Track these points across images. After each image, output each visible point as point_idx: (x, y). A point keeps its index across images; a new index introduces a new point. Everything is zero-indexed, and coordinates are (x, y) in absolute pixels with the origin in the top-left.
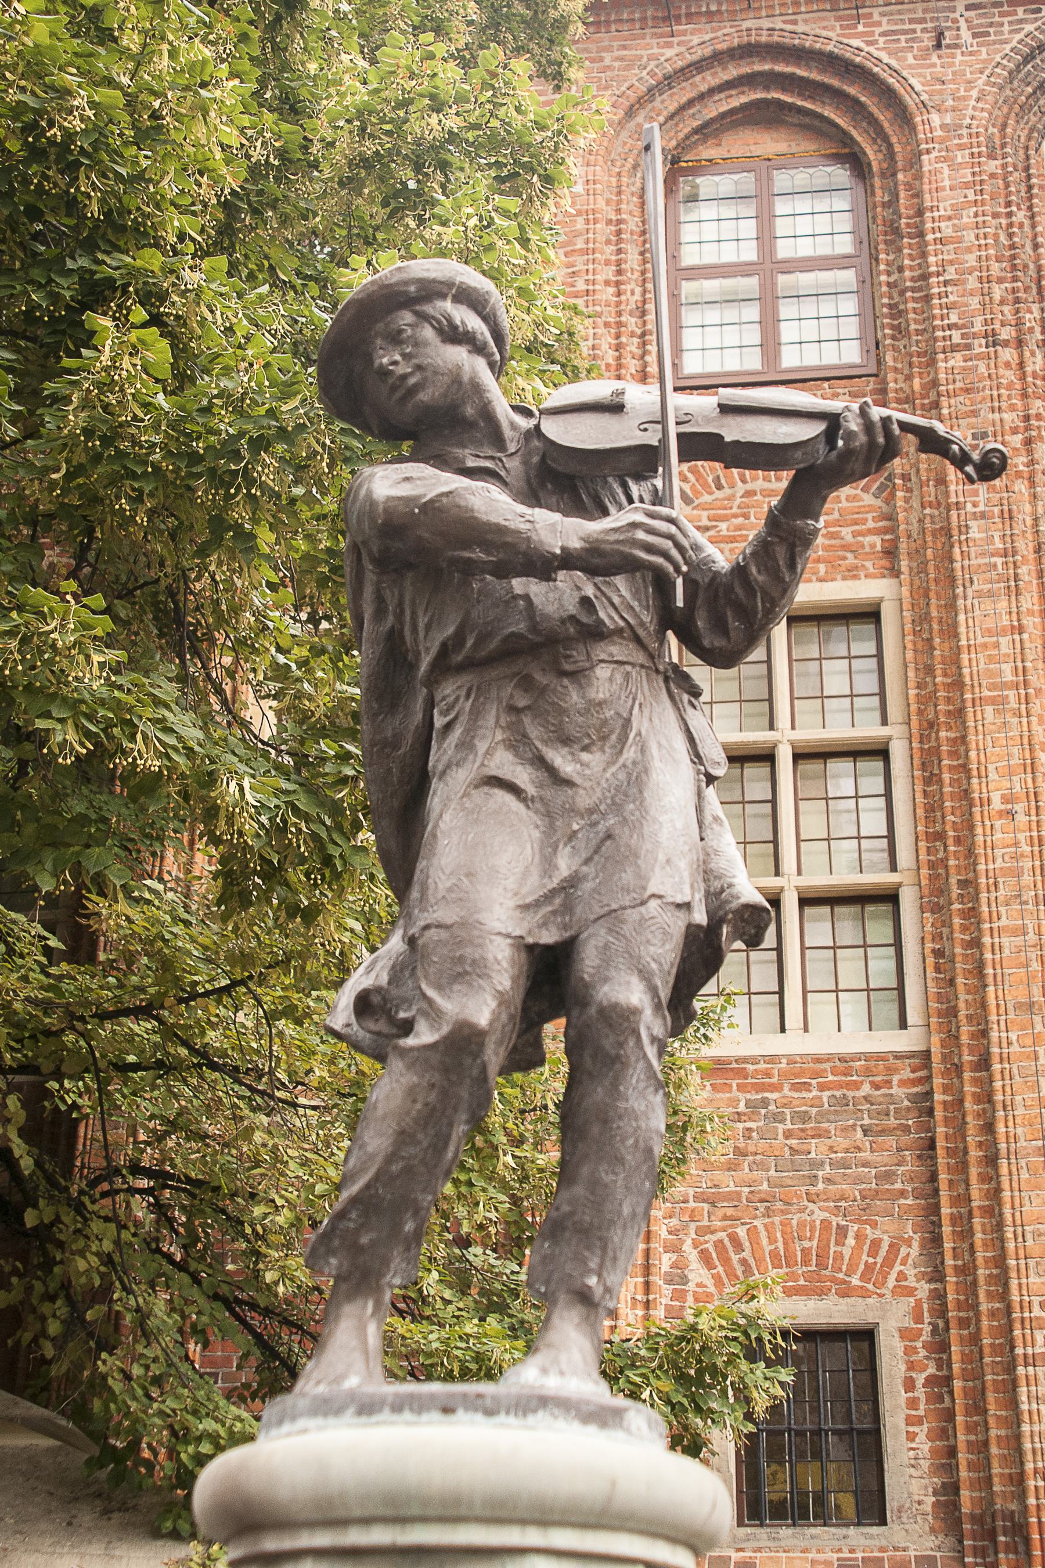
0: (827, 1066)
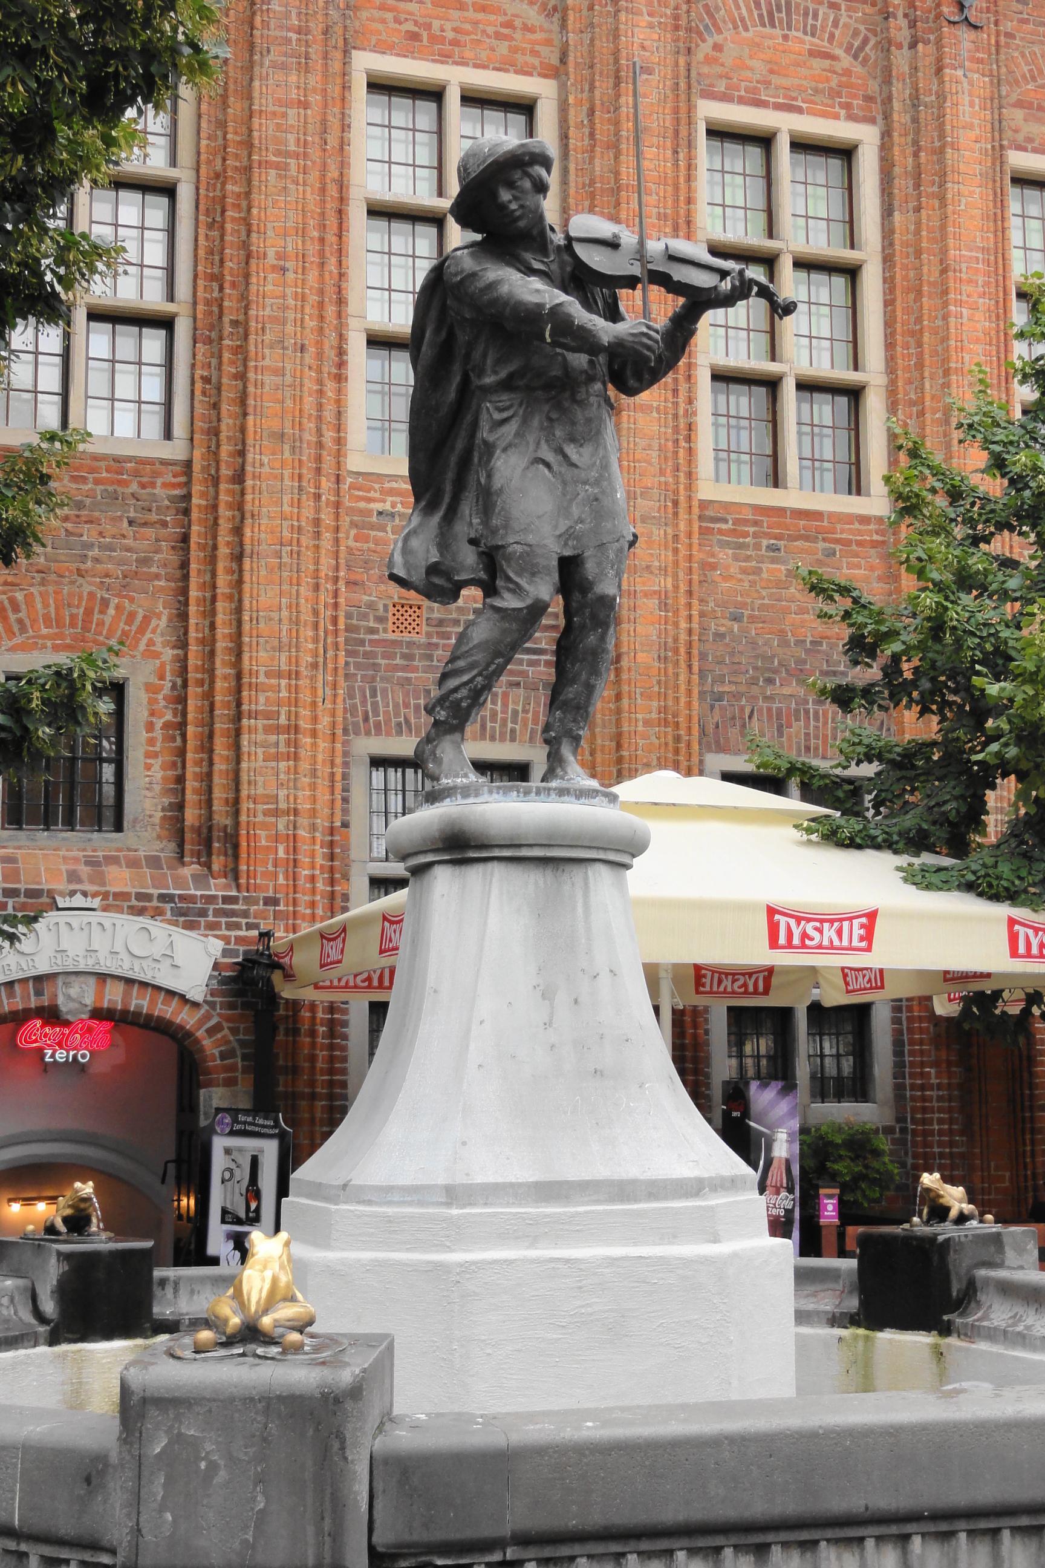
0: (103, 464)
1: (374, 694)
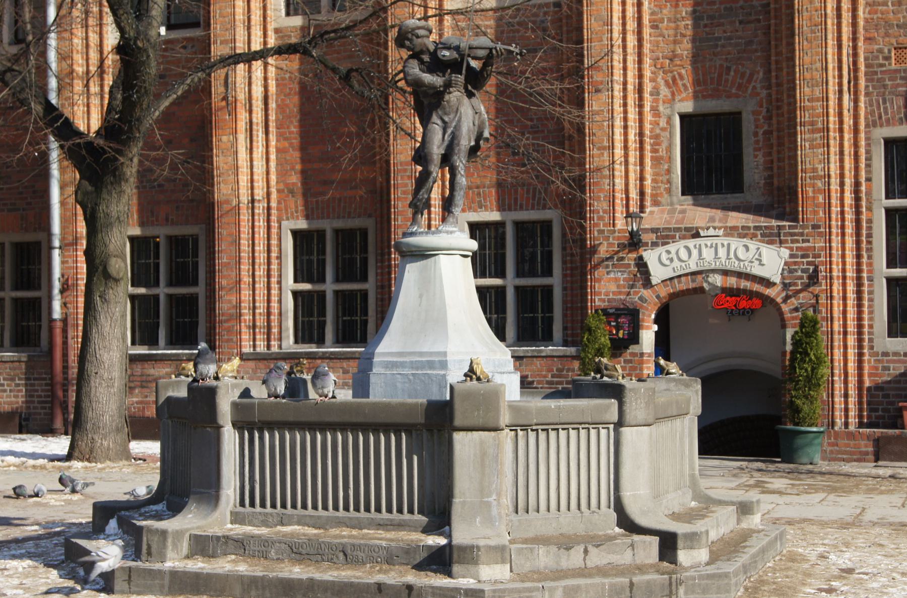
1: (884, 102)
